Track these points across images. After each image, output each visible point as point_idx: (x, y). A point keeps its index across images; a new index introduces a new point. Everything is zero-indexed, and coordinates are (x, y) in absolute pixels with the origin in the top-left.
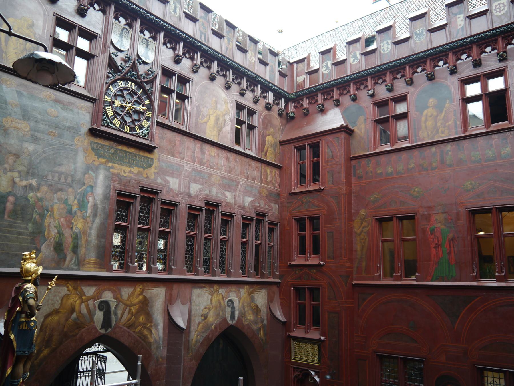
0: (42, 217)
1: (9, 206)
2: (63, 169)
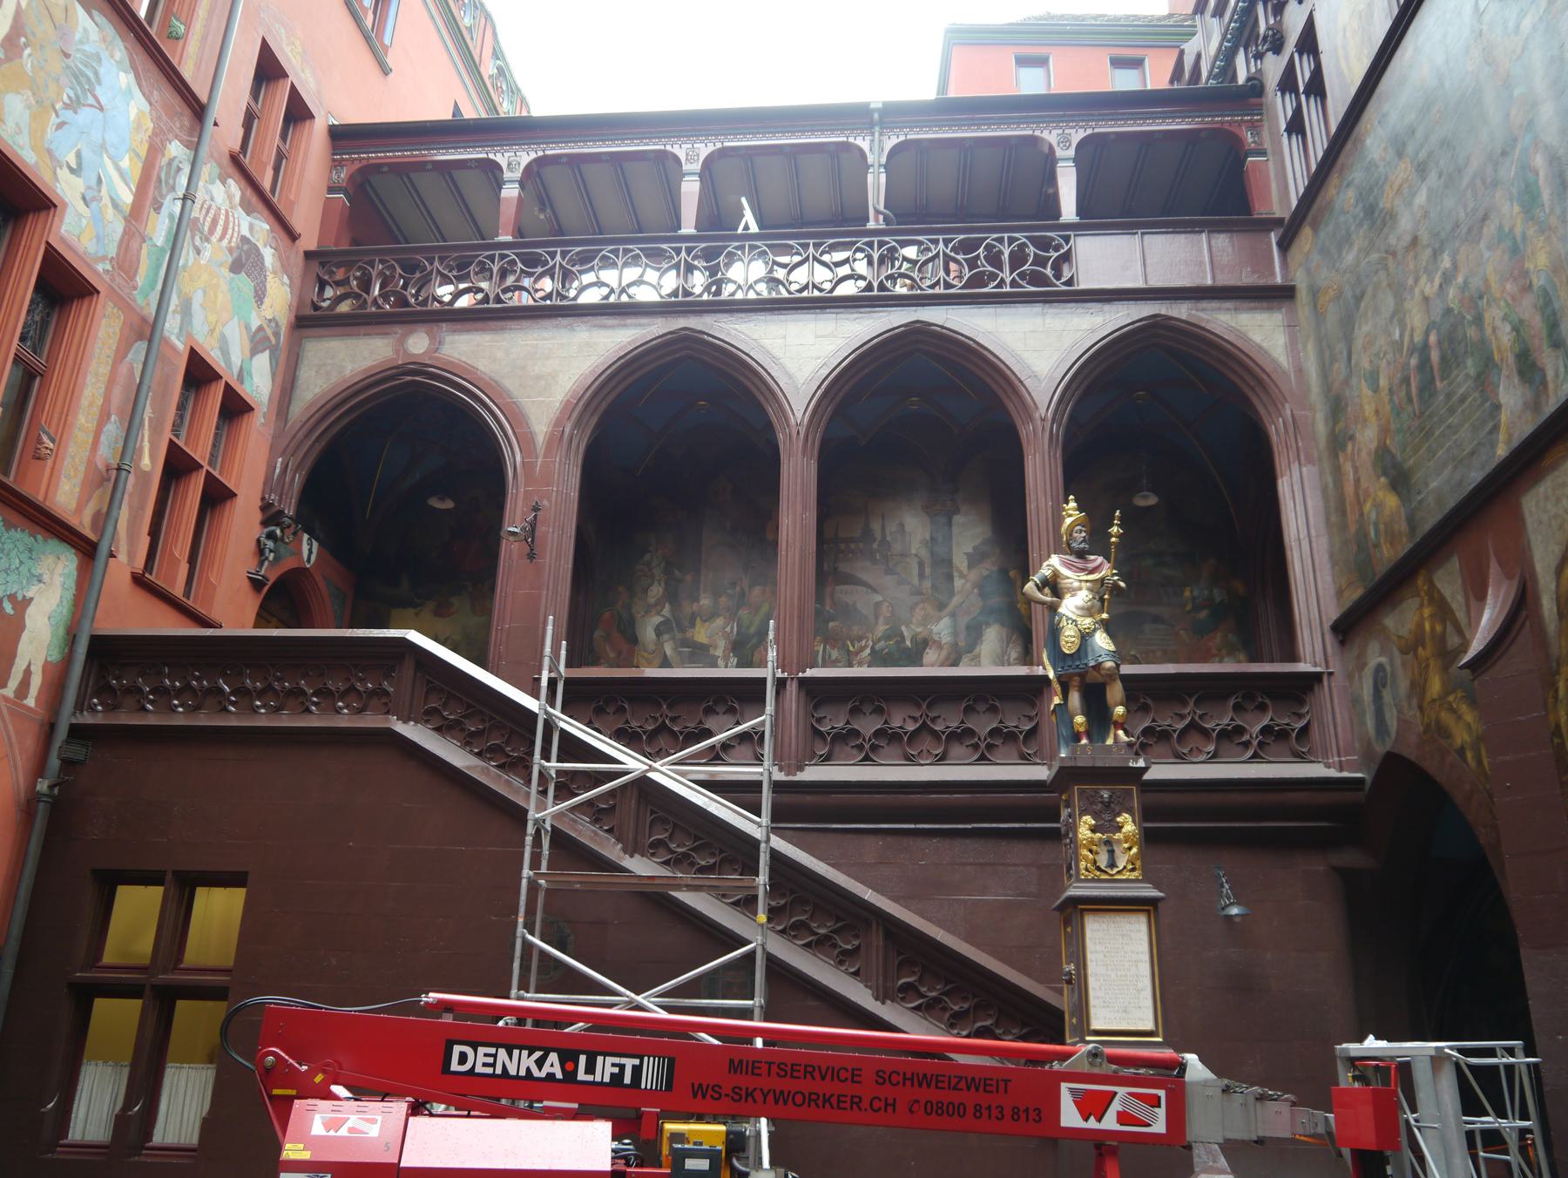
0: (1479, 320)
1: (1435, 356)
2: (1475, 164)
